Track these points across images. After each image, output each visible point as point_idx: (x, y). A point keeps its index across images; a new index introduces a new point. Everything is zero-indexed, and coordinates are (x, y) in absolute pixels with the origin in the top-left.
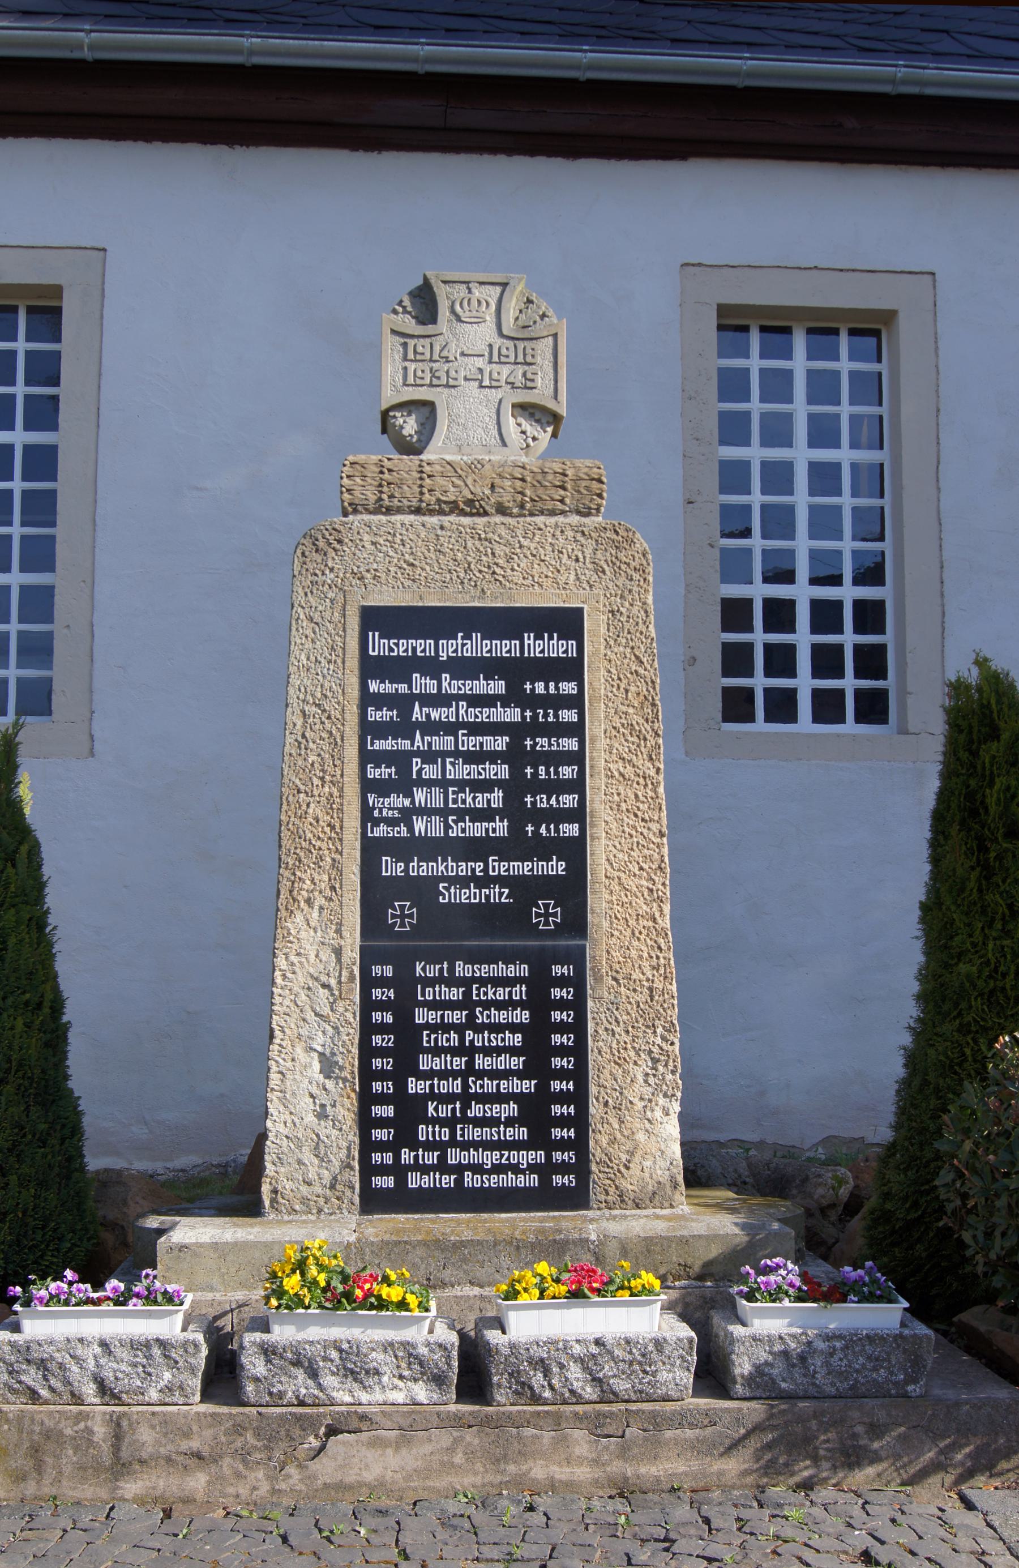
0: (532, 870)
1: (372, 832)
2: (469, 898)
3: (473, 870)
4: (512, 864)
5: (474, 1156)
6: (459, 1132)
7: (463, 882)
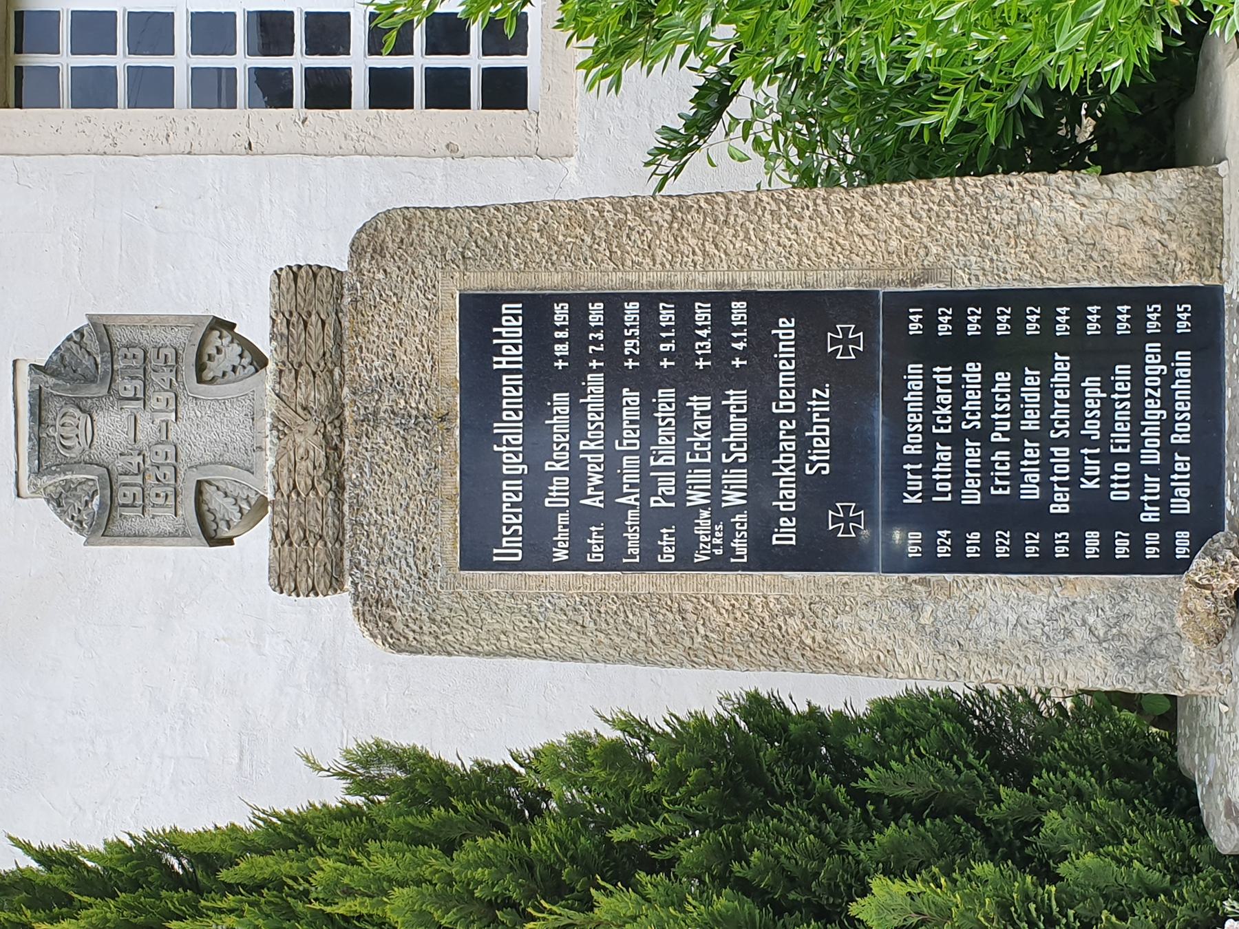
0: (789, 360)
1: (742, 557)
2: (823, 438)
3: (789, 432)
4: (781, 385)
5: (1151, 432)
6: (1120, 450)
7: (804, 447)
